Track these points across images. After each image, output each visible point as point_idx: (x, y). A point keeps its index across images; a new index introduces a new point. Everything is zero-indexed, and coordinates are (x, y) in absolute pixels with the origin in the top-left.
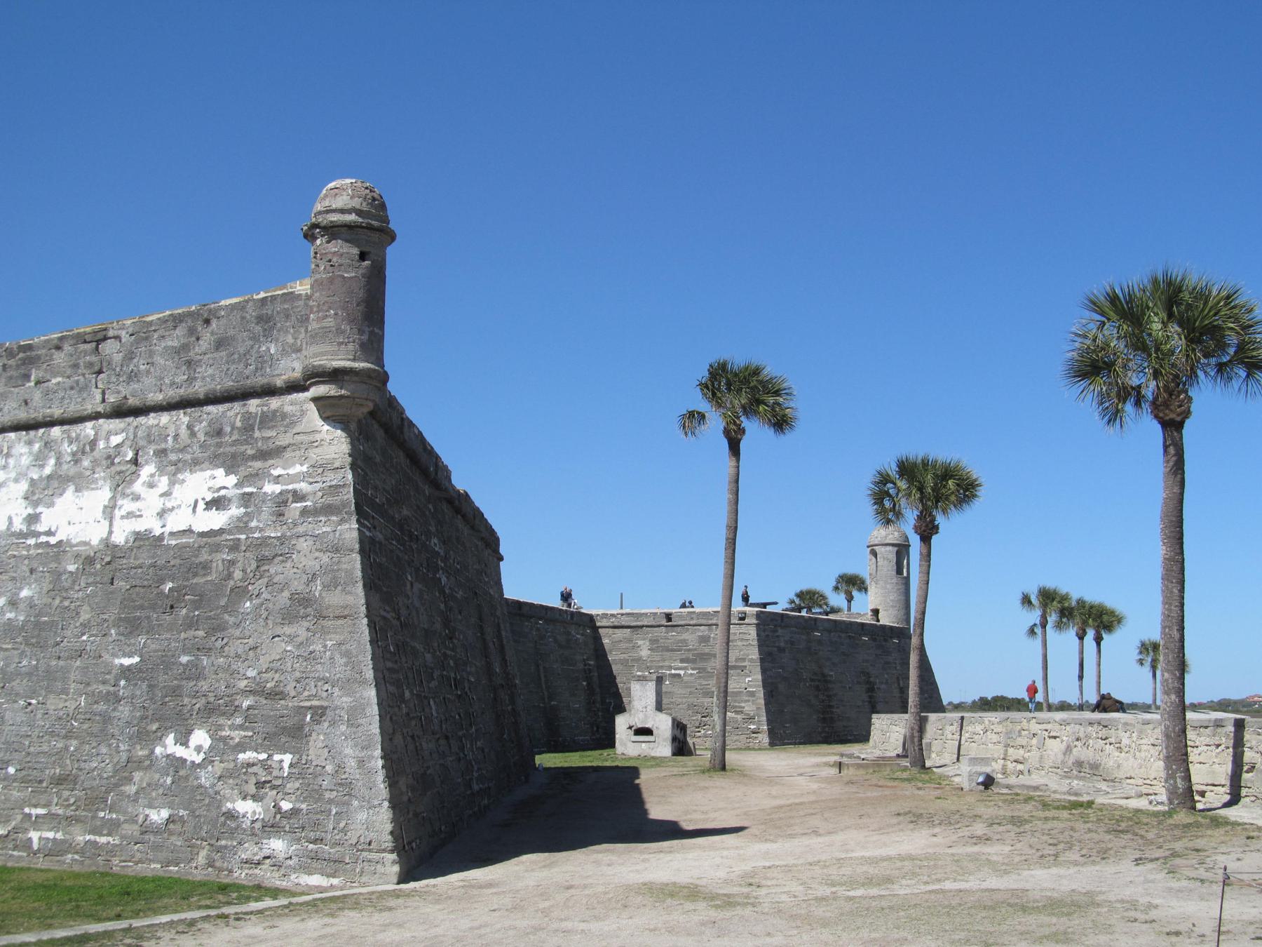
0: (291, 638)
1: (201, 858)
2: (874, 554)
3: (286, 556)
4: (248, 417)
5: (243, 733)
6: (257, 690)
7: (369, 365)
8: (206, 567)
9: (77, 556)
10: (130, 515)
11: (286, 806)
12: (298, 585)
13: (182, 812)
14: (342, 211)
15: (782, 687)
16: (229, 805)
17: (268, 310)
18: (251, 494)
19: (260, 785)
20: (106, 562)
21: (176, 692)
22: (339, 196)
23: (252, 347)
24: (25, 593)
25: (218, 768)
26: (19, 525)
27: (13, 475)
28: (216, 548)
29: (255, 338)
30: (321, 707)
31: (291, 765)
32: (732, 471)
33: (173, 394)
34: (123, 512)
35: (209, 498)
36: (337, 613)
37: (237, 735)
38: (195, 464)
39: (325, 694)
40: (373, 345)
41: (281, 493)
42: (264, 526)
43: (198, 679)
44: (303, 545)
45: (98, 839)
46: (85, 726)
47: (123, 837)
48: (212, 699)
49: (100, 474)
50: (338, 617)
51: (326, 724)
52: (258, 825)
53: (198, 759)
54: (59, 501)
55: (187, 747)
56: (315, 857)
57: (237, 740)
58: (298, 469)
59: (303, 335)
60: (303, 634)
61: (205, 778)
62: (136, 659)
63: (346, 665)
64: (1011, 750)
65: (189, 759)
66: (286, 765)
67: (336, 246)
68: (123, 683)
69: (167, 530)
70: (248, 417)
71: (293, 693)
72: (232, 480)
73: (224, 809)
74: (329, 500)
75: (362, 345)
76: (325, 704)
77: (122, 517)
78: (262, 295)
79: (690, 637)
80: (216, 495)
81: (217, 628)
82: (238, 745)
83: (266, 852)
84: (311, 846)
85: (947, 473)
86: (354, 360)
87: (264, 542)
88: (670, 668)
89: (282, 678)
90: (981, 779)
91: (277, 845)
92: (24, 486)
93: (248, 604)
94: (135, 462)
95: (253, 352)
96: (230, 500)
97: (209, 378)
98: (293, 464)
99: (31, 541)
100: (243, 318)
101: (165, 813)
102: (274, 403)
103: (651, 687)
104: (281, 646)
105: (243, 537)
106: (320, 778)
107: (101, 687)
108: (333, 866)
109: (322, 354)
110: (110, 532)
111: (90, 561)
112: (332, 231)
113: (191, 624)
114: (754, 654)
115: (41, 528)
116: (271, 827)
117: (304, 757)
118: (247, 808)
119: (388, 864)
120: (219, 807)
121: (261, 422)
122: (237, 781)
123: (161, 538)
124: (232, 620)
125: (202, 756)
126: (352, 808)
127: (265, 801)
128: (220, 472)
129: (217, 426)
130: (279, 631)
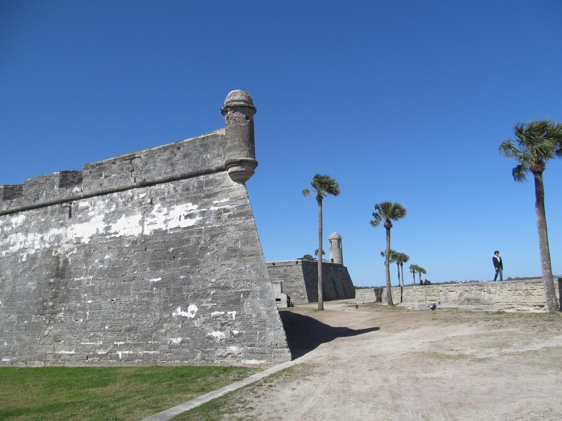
0: (230, 265)
1: (199, 356)
2: (331, 242)
3: (223, 234)
4: (199, 182)
6: (217, 287)
7: (250, 159)
8: (188, 241)
9: (129, 241)
10: (151, 223)
11: (236, 332)
12: (231, 244)
14: (238, 101)
15: (310, 284)
16: (209, 334)
17: (205, 142)
18: (205, 211)
19: (222, 325)
20: (142, 243)
21: (179, 290)
22: (235, 96)
23: (199, 156)
24: (107, 257)
25: (202, 319)
26: (101, 231)
27: (97, 212)
28: (192, 233)
29: (200, 153)
30: (247, 291)
31: (236, 316)
32: (320, 211)
33: (165, 176)
34: (148, 223)
35: (186, 214)
37: (210, 305)
38: (178, 202)
39: (248, 286)
40: (252, 152)
41: (218, 210)
42: (211, 222)
43: (189, 284)
44: (231, 229)
45: (149, 352)
46: (139, 307)
47: (161, 351)
48: (196, 292)
49: (136, 209)
50: (250, 256)
51: (250, 298)
52: (224, 341)
53: (193, 316)
54: (119, 221)
55: (187, 312)
56: (252, 352)
57: (210, 307)
58: (225, 200)
59: (222, 150)
61: (196, 324)
62: (160, 279)
63: (256, 274)
64: (428, 297)
65: (189, 317)
66: (234, 316)
67: (237, 114)
68: (155, 288)
69: (169, 228)
70: (199, 182)
71: (233, 287)
72: (196, 207)
73: (207, 336)
74: (240, 211)
75: (249, 151)
76: (249, 290)
77: (148, 225)
78: (202, 136)
79: (281, 270)
81: (195, 264)
82: (210, 309)
83: (229, 352)
84: (249, 348)
85: (396, 207)
86: (247, 157)
87: (213, 229)
88: (275, 280)
90: (431, 307)
91: (233, 349)
92: (103, 216)
93: (208, 253)
94: (151, 203)
95: (200, 158)
96: (195, 214)
97: (181, 169)
98: (223, 199)
99: (108, 237)
100: (195, 146)
101: (180, 339)
102: (211, 176)
103: (279, 285)
104: (225, 269)
105: (203, 228)
106: (250, 320)
107: (145, 291)
108: (261, 355)
109: (234, 155)
110: (143, 231)
111: (135, 242)
112: (235, 108)
113: (183, 263)
114: (302, 274)
115: (111, 231)
117: (242, 312)
118: (217, 334)
119: (286, 353)
120: (205, 335)
121: (206, 184)
123: (166, 231)
124: (202, 260)
125: (194, 315)
126: (267, 331)
127: (226, 331)
128: (190, 204)
129: (186, 187)
130: (224, 263)
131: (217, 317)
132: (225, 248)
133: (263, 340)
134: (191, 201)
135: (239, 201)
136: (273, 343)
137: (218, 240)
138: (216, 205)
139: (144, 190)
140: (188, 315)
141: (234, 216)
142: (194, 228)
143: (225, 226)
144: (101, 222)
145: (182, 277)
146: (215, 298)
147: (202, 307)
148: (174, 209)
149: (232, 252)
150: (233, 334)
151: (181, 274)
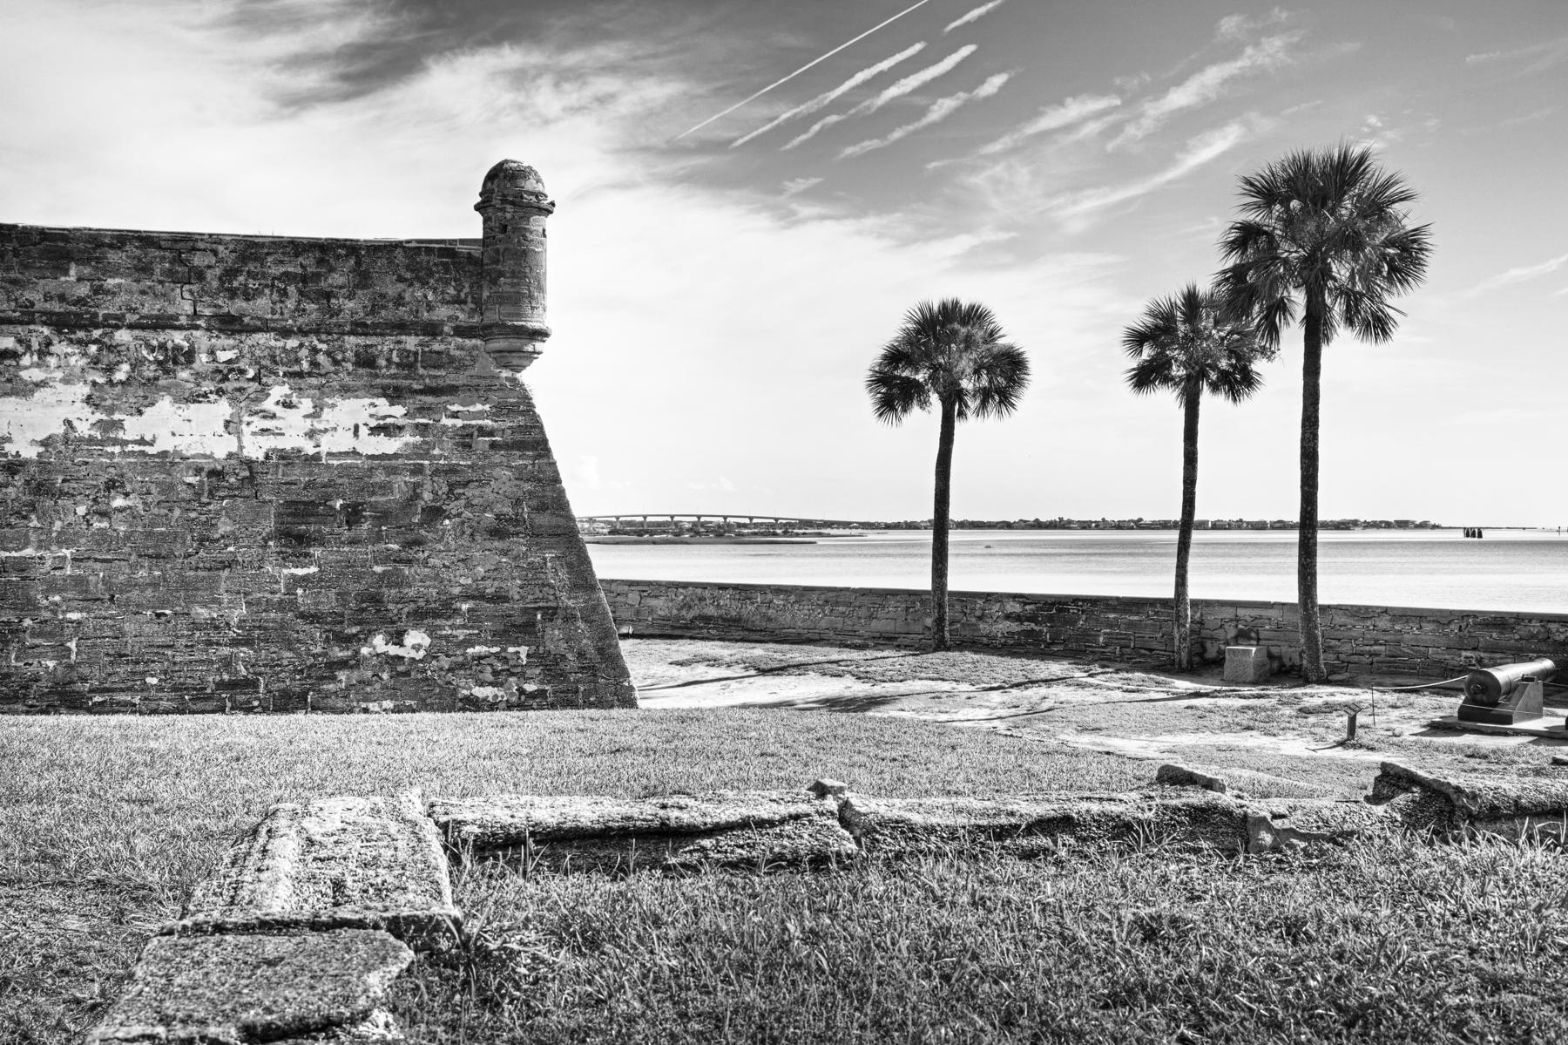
8: (385, 488)
11: (530, 687)
16: (466, 692)
18: (426, 425)
19: (495, 673)
25: (445, 662)
27: (59, 375)
28: (393, 471)
31: (528, 656)
34: (253, 428)
35: (373, 423)
37: (461, 634)
41: (464, 427)
42: (445, 453)
58: (479, 407)
66: (523, 656)
68: (300, 591)
69: (324, 449)
71: (517, 597)
72: (399, 410)
74: (518, 437)
87: (453, 470)
98: (473, 403)
111: (213, 473)
123: (317, 457)
124: (430, 536)
125: (422, 653)
128: (382, 402)
131: (481, 658)
134: (385, 396)
137: (469, 493)
138: (455, 415)
139: (231, 342)
141: (507, 446)
142: (400, 461)
144: (79, 404)
145: (378, 569)
146: (474, 618)
147: (441, 637)
148: (333, 406)
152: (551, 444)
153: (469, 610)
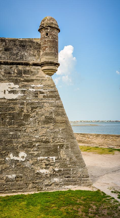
3: (41, 108)
5: (37, 152)
8: (13, 109)
11: (57, 169)
13: (20, 175)
18: (25, 90)
19: (46, 165)
21: (11, 142)
25: (31, 162)
28: (16, 104)
30: (62, 145)
31: (56, 159)
35: (10, 90)
36: (61, 122)
37: (36, 153)
39: (62, 141)
42: (30, 98)
52: (48, 175)
53: (23, 160)
59: (36, 52)
60: (52, 127)
61: (28, 164)
66: (54, 159)
72: (17, 86)
73: (36, 172)
74: (51, 94)
76: (63, 144)
80: (12, 90)
82: (36, 155)
83: (53, 182)
84: (66, 179)
87: (32, 103)
89: (48, 138)
91: (56, 180)
95: (19, 54)
98: (38, 84)
101: (14, 176)
102: (28, 68)
105: (25, 101)
116: (54, 175)
117: (59, 157)
122: (38, 165)
124: (26, 123)
125: (24, 159)
127: (49, 169)
128: (12, 84)
130: (43, 126)
132: (43, 117)
133: (75, 174)
134: (13, 82)
135: (50, 88)
136: (81, 175)
138: (33, 88)
140: (20, 159)
142: (17, 101)
143: (41, 103)
145: (11, 133)
147: (30, 154)
149: (48, 120)
150: (55, 171)
151: (11, 131)
152: (61, 96)
153: (38, 146)
